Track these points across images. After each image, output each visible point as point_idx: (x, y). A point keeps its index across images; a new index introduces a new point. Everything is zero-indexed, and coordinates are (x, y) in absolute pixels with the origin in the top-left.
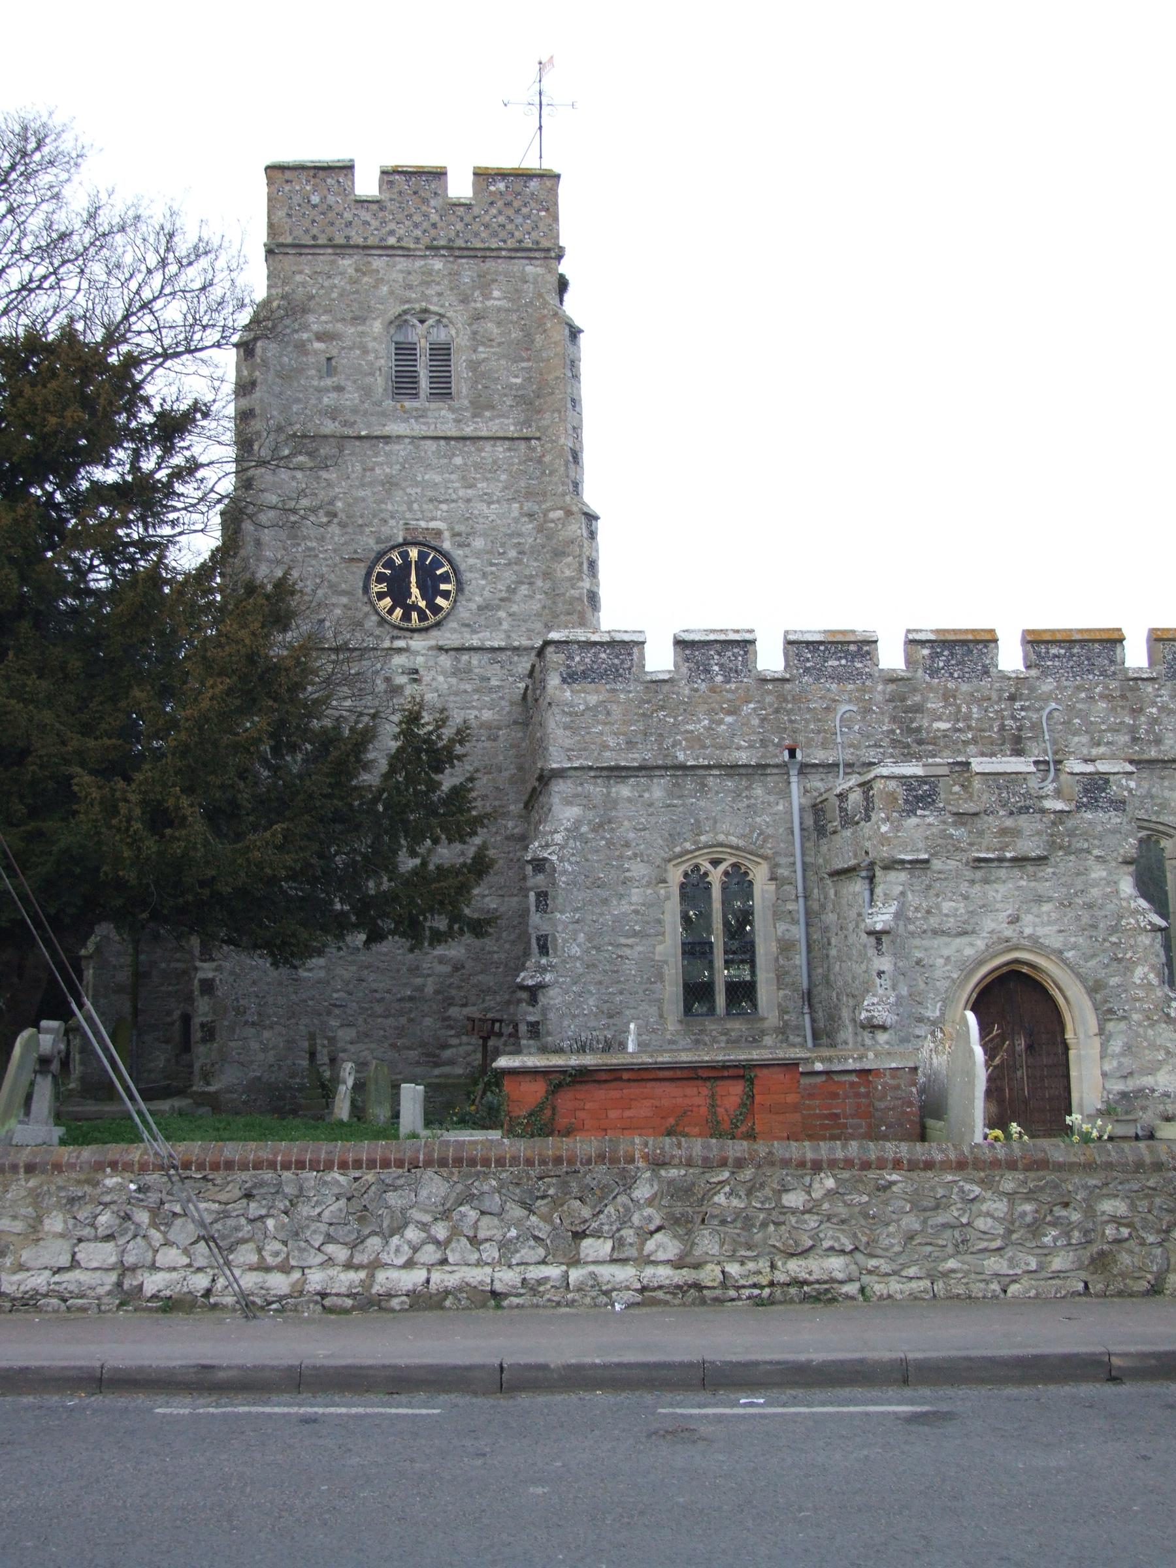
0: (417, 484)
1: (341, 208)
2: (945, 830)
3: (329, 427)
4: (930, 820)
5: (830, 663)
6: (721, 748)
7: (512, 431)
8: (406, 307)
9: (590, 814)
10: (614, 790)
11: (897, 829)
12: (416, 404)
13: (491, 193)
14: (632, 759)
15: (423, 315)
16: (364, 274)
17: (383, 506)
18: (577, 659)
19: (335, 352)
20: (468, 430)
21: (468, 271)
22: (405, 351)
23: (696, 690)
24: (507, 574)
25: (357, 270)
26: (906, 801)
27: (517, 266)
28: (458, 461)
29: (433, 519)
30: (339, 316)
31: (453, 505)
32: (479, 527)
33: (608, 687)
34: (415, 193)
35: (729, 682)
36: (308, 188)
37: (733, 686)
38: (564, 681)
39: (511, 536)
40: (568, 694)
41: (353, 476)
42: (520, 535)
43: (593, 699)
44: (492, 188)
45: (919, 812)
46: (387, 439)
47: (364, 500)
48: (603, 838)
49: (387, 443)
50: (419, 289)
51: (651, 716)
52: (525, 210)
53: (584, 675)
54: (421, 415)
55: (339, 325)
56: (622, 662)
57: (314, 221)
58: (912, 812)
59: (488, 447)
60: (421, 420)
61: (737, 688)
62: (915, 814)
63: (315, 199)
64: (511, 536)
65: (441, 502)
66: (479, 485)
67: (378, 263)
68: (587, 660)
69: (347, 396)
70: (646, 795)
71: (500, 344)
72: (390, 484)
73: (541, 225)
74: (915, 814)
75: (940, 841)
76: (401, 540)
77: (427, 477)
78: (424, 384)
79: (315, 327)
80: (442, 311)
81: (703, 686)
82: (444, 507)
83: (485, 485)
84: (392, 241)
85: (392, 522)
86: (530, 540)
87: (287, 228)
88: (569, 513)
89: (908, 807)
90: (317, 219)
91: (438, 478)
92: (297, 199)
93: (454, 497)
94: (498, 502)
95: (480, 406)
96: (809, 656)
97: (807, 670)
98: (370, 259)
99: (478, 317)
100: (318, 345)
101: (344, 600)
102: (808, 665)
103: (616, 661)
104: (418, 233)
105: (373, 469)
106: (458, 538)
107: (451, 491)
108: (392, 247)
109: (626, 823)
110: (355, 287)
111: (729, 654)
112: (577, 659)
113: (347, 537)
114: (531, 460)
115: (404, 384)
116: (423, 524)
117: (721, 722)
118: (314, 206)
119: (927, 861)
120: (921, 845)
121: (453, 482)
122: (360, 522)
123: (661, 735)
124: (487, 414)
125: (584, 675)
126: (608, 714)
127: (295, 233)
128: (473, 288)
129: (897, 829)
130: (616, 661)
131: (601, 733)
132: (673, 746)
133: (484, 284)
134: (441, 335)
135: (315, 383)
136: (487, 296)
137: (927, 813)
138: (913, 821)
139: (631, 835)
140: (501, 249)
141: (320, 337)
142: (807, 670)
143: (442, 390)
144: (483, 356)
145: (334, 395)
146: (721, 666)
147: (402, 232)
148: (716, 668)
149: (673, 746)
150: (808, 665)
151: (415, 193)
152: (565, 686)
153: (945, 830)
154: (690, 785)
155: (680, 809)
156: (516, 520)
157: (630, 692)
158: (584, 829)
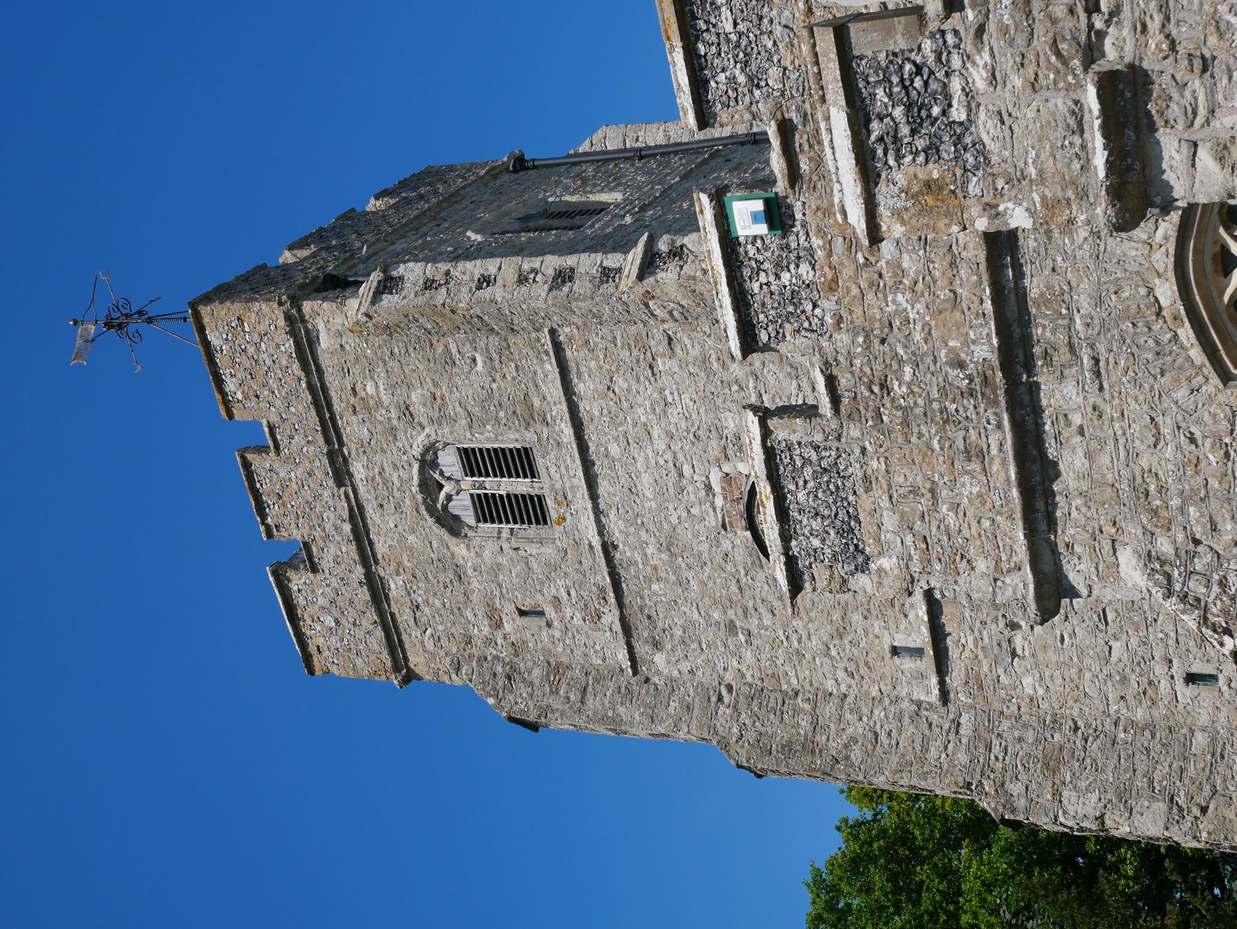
0: (662, 508)
1: (327, 589)
2: (1004, 30)
3: (611, 617)
4: (979, 78)
5: (729, 27)
6: (953, 264)
7: (551, 367)
8: (423, 509)
9: (1133, 530)
10: (1072, 484)
11: (1017, 179)
12: (550, 503)
13: (246, 397)
14: (1000, 441)
15: (429, 487)
16: (399, 564)
17: (705, 556)
18: (816, 543)
19: (509, 608)
20: (568, 431)
21: (353, 429)
22: (488, 508)
23: (839, 320)
24: (772, 381)
25: (398, 574)
26: (932, 151)
27: (325, 360)
28: (614, 450)
29: (708, 487)
30: (461, 598)
31: (680, 456)
32: (707, 419)
33: (860, 491)
34: (280, 497)
35: (811, 251)
36: (319, 628)
37: (816, 242)
38: (863, 568)
39: (710, 373)
40: (885, 563)
41: (671, 596)
42: (705, 360)
43: (890, 521)
44: (240, 396)
45: (958, 113)
46: (608, 549)
47: (703, 583)
48: (1181, 509)
49: (615, 547)
50: (397, 494)
51: (906, 410)
52: (251, 350)
53: (846, 531)
54: (564, 500)
55: (474, 597)
56: (807, 461)
57: (354, 624)
58: (960, 132)
59: (584, 406)
60: (570, 496)
61: (821, 232)
62: (966, 126)
63: (329, 621)
64: (710, 373)
65: (681, 475)
66: (643, 419)
67: (381, 548)
68: (816, 524)
69: (565, 595)
70: (1077, 419)
71: (436, 385)
72: (669, 546)
73: (262, 328)
74: (966, 126)
75: (1042, 41)
76: (748, 534)
77: (648, 494)
78: (520, 486)
79: (486, 630)
80: (416, 466)
81: (828, 304)
82: (687, 470)
83: (640, 411)
84: (347, 527)
85: (726, 545)
86: (710, 342)
87: (373, 657)
88: (648, 296)
89: (948, 151)
90: (351, 620)
91: (646, 479)
92: (334, 640)
93: (669, 456)
94: (661, 391)
95: (531, 416)
96: (722, 77)
97: (754, 82)
98: (379, 556)
99: (406, 411)
100: (508, 627)
101: (856, 618)
102: (742, 79)
103: (808, 472)
104: (326, 494)
105: (655, 568)
106: (730, 452)
107: (662, 462)
108: (355, 531)
109: (1144, 462)
110: (419, 575)
111: (752, 251)
112: (816, 543)
113: (762, 610)
114: (587, 342)
115: (531, 511)
116: (719, 502)
117: (896, 266)
118: (337, 622)
119: (1109, 84)
120: (1060, 103)
121: (647, 458)
122: (734, 589)
123: (942, 391)
124: (537, 402)
125: (846, 531)
126: (915, 491)
127: (376, 647)
128: (374, 422)
129: (1017, 179)
130: (808, 472)
131: (956, 507)
132: (961, 365)
133: (365, 407)
134: (449, 462)
135: (557, 634)
136: (379, 403)
137: (956, 85)
138: (986, 129)
139: (1169, 452)
140: (311, 387)
141: (499, 625)
142: (754, 82)
143: (520, 462)
144: (458, 409)
145: (568, 612)
146: (779, 267)
147: (332, 516)
148: (786, 277)
149: (961, 365)
150: (742, 79)
151: (280, 497)
152: (873, 566)
153: (1004, 30)
154: (1042, 332)
155: (1101, 348)
156: (683, 364)
157: (863, 451)
158: (1164, 546)
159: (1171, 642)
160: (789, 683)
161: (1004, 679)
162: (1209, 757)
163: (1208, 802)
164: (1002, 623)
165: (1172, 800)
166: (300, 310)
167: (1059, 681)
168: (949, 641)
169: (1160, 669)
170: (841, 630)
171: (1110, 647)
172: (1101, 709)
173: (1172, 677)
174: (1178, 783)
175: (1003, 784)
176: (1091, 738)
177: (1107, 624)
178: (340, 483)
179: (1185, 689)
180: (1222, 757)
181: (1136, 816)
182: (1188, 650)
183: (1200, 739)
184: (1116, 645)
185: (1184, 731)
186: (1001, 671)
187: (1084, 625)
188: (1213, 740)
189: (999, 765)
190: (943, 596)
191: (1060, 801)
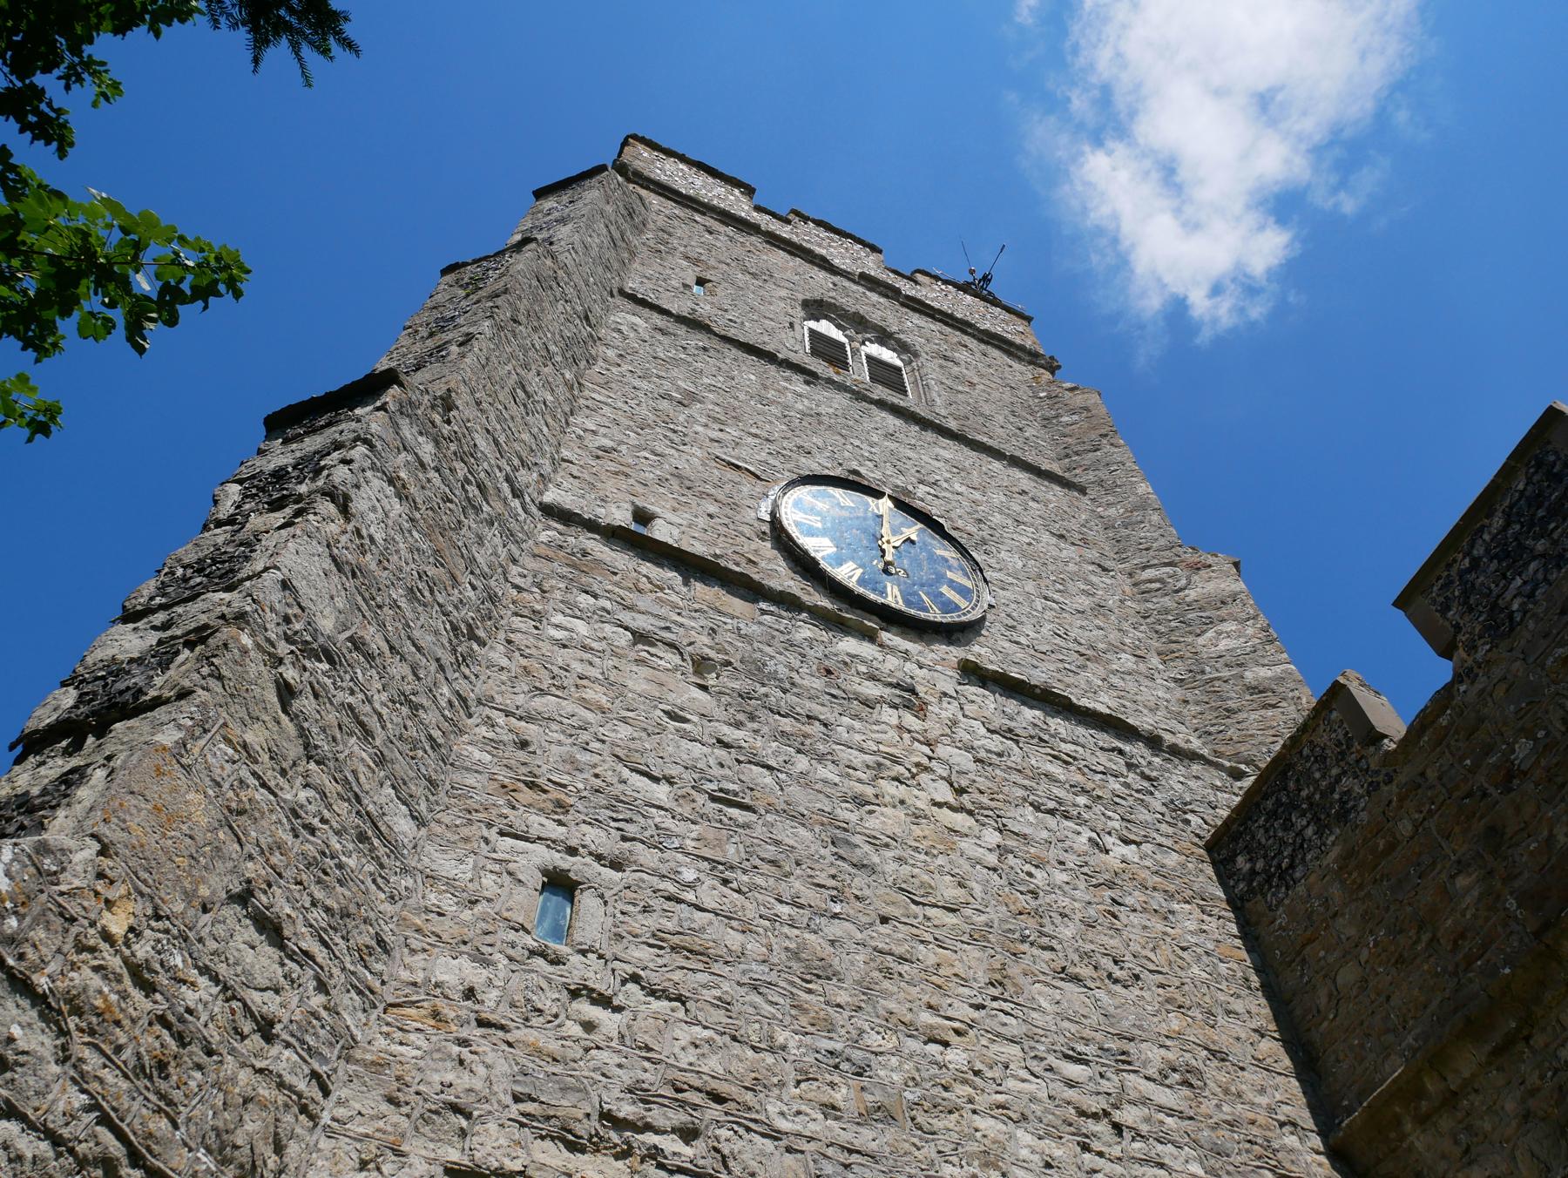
159: (671, 888)
160: (594, 391)
161: (585, 600)
162: (371, 808)
163: (293, 718)
164: (712, 654)
165: (331, 661)
166: (1042, 366)
167: (578, 667)
168: (673, 577)
169: (601, 839)
170: (688, 483)
171: (656, 780)
172: (499, 699)
173: (572, 851)
174: (350, 700)
175: (437, 443)
176: (455, 641)
177: (714, 799)
178: (863, 276)
179: (538, 861)
180: (362, 837)
181: (328, 564)
182: (646, 910)
183: (403, 826)
184: (661, 792)
185: (423, 807)
186: (608, 605)
187: (712, 762)
188: (394, 848)
189: (460, 474)
190: (764, 612)
191: (391, 482)
